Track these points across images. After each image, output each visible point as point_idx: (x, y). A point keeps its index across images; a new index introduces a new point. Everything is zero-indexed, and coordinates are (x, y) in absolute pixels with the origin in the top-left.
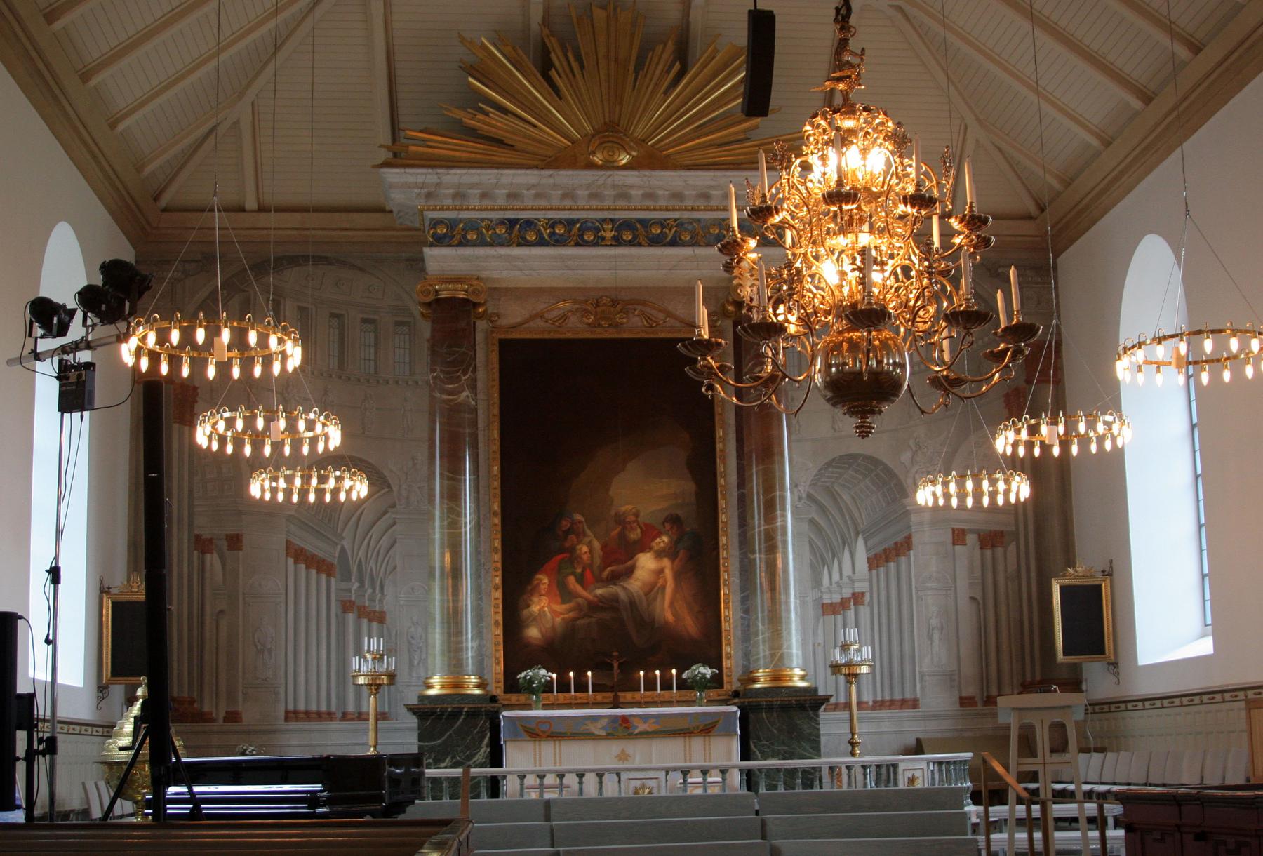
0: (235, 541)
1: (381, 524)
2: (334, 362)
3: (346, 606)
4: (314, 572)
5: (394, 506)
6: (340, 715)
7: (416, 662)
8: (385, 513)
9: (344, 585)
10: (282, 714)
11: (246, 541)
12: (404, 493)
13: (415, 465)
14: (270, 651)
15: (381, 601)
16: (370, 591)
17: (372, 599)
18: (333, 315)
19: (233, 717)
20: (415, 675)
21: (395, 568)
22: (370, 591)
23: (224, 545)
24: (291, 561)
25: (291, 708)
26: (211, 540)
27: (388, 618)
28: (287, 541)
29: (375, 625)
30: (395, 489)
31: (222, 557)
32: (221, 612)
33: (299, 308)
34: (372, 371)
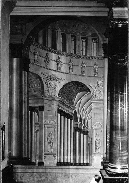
0: (42, 108)
1: (87, 104)
2: (73, 52)
3: (76, 129)
4: (66, 118)
5: (91, 98)
6: (73, 164)
7: (98, 148)
8: (89, 100)
9: (76, 123)
10: (56, 163)
11: (45, 108)
12: (94, 94)
13: (98, 85)
14: (52, 143)
15: (87, 128)
16: (84, 125)
17: (84, 127)
18: (72, 36)
19: (41, 164)
20: (97, 151)
21: (91, 118)
22: (84, 125)
23: (38, 109)
24: (59, 115)
25: (59, 161)
26: (34, 108)
27: (89, 134)
28: (58, 109)
29: (85, 136)
30: (92, 92)
31: (38, 113)
32: (37, 131)
33: (62, 34)
34: (85, 55)
